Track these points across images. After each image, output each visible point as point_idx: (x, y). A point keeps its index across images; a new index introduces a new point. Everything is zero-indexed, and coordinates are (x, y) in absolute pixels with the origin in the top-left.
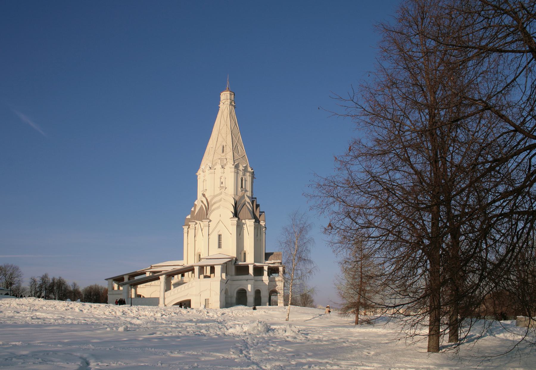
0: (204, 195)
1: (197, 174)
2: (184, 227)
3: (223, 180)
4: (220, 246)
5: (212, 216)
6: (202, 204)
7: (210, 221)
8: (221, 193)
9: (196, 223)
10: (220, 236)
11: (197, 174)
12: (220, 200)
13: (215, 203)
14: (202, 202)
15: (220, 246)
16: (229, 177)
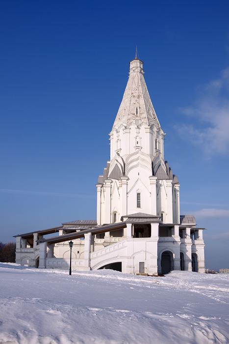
0: (118, 154)
1: (110, 135)
2: (97, 186)
3: (138, 140)
4: (139, 206)
5: (130, 174)
6: (116, 162)
7: (128, 179)
8: (137, 153)
9: (112, 182)
10: (139, 194)
11: (110, 135)
12: (137, 159)
13: (132, 162)
14: (117, 160)
15: (139, 206)
16: (145, 137)
